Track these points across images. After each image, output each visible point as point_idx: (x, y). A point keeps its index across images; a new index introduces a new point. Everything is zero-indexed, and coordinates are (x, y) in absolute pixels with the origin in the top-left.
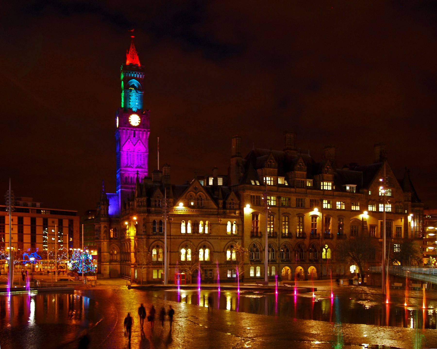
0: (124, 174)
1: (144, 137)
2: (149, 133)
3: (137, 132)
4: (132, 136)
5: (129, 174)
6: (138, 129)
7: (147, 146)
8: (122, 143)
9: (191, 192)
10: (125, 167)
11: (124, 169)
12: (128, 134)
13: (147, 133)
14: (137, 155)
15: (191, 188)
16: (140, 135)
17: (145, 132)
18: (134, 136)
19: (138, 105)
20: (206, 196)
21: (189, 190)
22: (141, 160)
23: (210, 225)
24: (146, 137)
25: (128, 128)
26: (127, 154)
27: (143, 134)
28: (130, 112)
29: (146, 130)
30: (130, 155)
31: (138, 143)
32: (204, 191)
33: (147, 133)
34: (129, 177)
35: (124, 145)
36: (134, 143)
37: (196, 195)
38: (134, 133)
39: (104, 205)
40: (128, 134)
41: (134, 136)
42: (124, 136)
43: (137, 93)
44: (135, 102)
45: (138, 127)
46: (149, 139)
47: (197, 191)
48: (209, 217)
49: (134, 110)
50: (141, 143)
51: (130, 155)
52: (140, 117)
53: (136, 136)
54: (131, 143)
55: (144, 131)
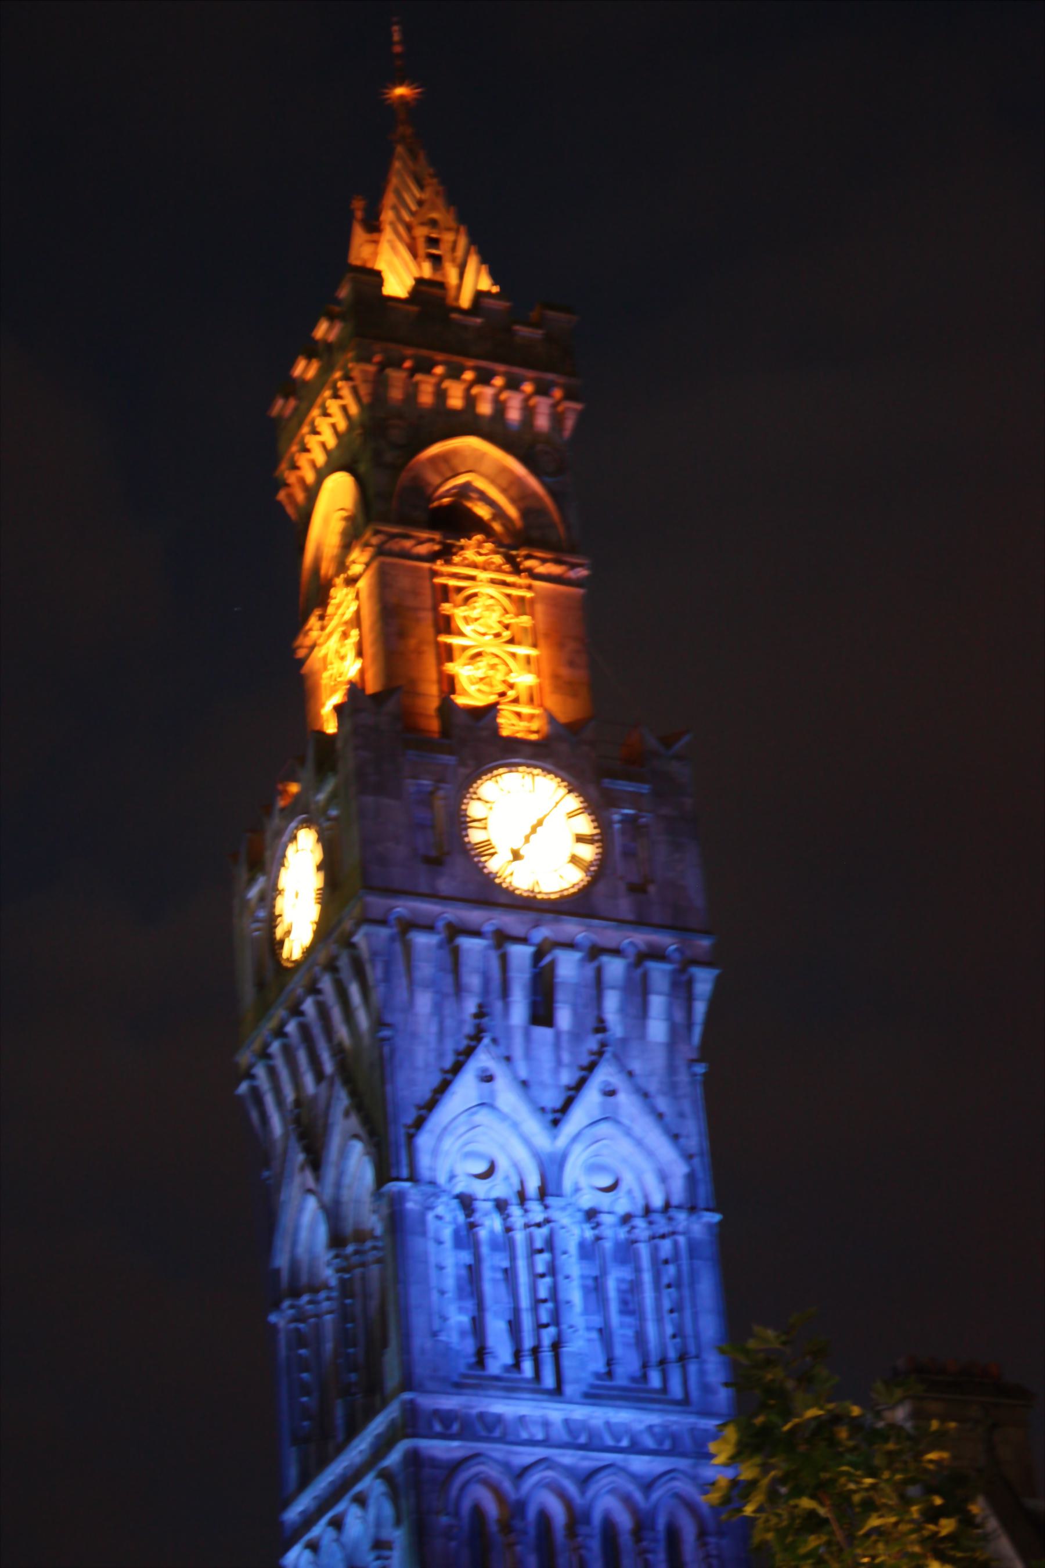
0: (456, 1466)
1: (657, 1030)
2: (704, 981)
3: (568, 967)
4: (519, 1011)
6: (572, 928)
7: (693, 1130)
10: (459, 1386)
11: (450, 1403)
12: (473, 981)
16: (612, 1002)
18: (542, 1013)
22: (630, 1305)
24: (677, 1033)
25: (474, 916)
26: (467, 1236)
27: (638, 991)
28: (477, 743)
30: (506, 1243)
31: (591, 1099)
33: (682, 989)
35: (431, 1104)
41: (542, 1013)
42: (424, 1002)
43: (517, 570)
44: (496, 648)
45: (573, 905)
46: (706, 1052)
50: (626, 1100)
53: (564, 1017)
54: (507, 1096)
55: (656, 954)
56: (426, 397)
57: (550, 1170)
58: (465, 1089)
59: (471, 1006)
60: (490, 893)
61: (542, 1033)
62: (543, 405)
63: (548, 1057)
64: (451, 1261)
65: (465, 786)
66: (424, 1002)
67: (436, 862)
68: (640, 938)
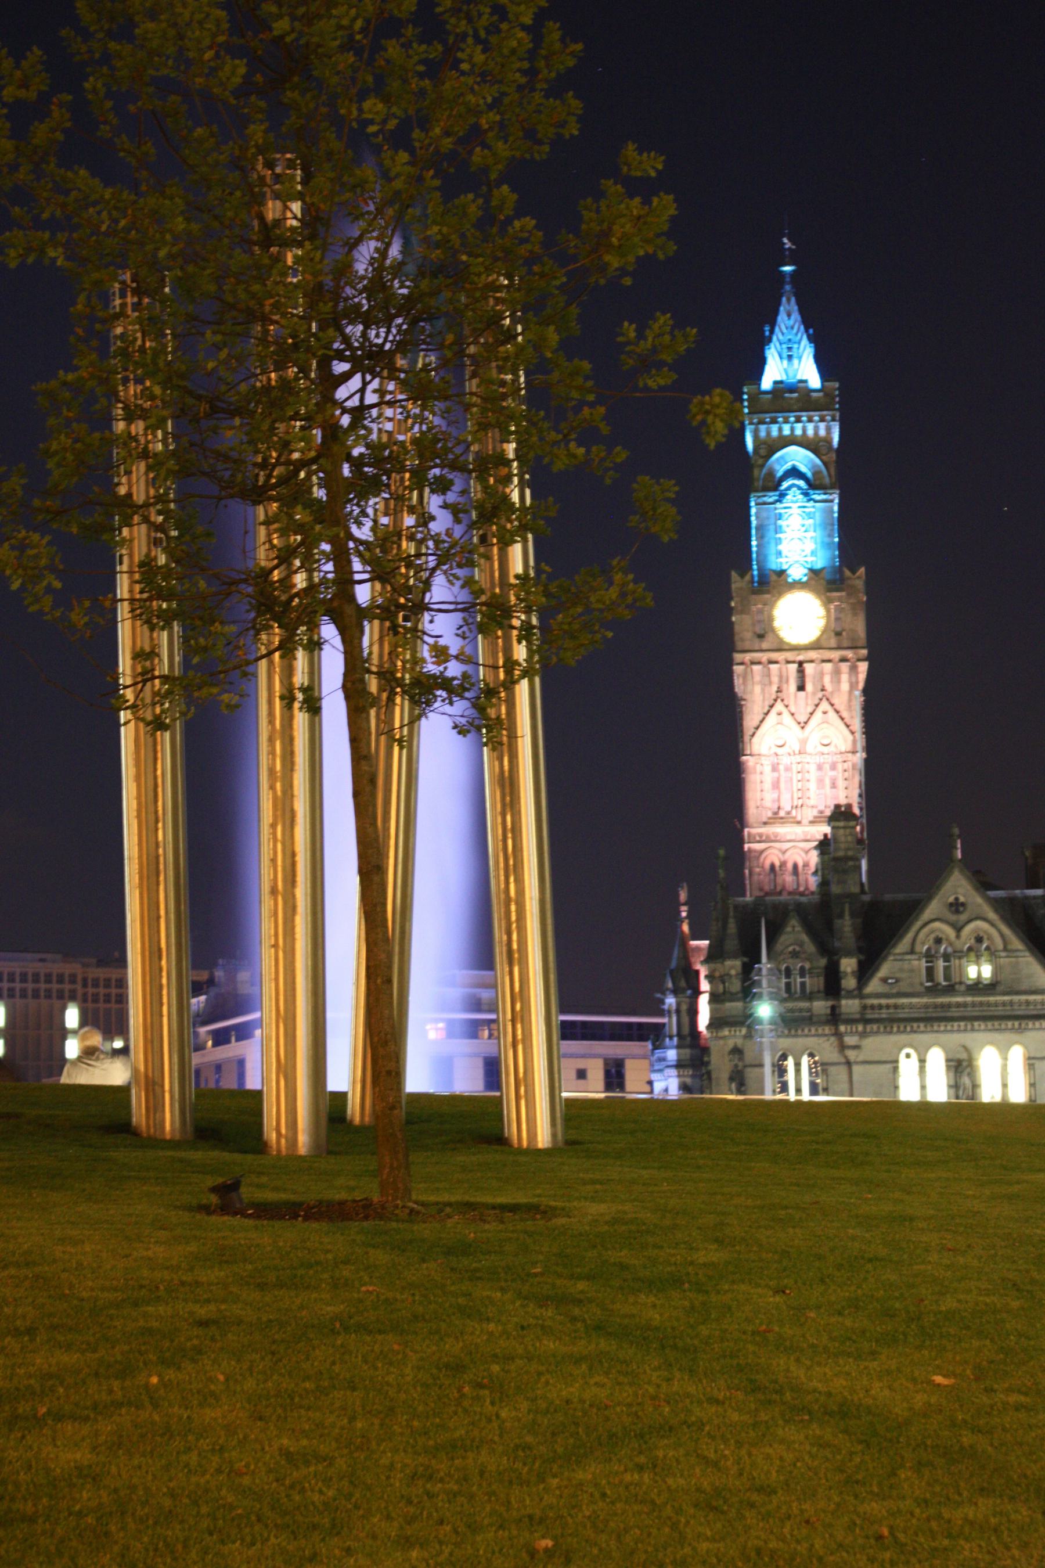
0: (762, 852)
1: (845, 686)
2: (863, 667)
3: (809, 668)
4: (793, 686)
5: (784, 852)
6: (813, 654)
7: (857, 724)
8: (750, 721)
9: (937, 925)
11: (763, 830)
13: (854, 669)
14: (820, 767)
15: (934, 908)
16: (827, 680)
17: (845, 667)
18: (801, 688)
19: (813, 553)
20: (1002, 935)
21: (928, 914)
22: (834, 786)
23: (1031, 1062)
24: (853, 686)
25: (774, 656)
26: (775, 768)
27: (837, 672)
29: (849, 654)
30: (788, 769)
31: (818, 715)
32: (992, 915)
33: (854, 669)
34: (783, 864)
36: (802, 718)
37: (958, 937)
38: (801, 671)
39: (675, 992)
40: (775, 679)
41: (801, 688)
42: (757, 689)
46: (865, 691)
47: (963, 917)
48: (1020, 1030)
49: (797, 573)
50: (832, 714)
51: (788, 769)
52: (827, 602)
53: (809, 687)
54: (786, 717)
55: (843, 660)
56: (775, 433)
57: (804, 742)
58: (772, 717)
59: (775, 688)
60: (781, 647)
61: (802, 693)
62: (822, 426)
63: (801, 703)
64: (768, 777)
65: (772, 605)
66: (757, 689)
67: (761, 636)
68: (836, 655)
